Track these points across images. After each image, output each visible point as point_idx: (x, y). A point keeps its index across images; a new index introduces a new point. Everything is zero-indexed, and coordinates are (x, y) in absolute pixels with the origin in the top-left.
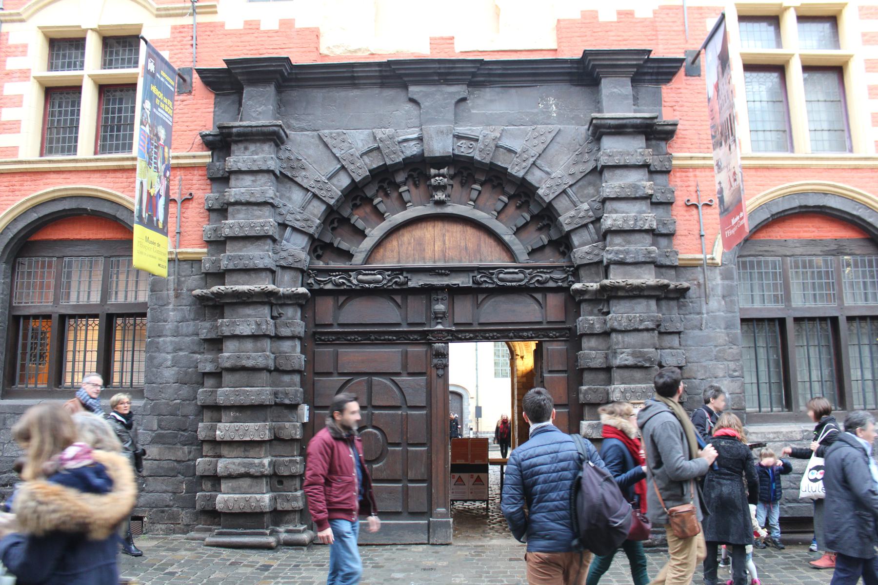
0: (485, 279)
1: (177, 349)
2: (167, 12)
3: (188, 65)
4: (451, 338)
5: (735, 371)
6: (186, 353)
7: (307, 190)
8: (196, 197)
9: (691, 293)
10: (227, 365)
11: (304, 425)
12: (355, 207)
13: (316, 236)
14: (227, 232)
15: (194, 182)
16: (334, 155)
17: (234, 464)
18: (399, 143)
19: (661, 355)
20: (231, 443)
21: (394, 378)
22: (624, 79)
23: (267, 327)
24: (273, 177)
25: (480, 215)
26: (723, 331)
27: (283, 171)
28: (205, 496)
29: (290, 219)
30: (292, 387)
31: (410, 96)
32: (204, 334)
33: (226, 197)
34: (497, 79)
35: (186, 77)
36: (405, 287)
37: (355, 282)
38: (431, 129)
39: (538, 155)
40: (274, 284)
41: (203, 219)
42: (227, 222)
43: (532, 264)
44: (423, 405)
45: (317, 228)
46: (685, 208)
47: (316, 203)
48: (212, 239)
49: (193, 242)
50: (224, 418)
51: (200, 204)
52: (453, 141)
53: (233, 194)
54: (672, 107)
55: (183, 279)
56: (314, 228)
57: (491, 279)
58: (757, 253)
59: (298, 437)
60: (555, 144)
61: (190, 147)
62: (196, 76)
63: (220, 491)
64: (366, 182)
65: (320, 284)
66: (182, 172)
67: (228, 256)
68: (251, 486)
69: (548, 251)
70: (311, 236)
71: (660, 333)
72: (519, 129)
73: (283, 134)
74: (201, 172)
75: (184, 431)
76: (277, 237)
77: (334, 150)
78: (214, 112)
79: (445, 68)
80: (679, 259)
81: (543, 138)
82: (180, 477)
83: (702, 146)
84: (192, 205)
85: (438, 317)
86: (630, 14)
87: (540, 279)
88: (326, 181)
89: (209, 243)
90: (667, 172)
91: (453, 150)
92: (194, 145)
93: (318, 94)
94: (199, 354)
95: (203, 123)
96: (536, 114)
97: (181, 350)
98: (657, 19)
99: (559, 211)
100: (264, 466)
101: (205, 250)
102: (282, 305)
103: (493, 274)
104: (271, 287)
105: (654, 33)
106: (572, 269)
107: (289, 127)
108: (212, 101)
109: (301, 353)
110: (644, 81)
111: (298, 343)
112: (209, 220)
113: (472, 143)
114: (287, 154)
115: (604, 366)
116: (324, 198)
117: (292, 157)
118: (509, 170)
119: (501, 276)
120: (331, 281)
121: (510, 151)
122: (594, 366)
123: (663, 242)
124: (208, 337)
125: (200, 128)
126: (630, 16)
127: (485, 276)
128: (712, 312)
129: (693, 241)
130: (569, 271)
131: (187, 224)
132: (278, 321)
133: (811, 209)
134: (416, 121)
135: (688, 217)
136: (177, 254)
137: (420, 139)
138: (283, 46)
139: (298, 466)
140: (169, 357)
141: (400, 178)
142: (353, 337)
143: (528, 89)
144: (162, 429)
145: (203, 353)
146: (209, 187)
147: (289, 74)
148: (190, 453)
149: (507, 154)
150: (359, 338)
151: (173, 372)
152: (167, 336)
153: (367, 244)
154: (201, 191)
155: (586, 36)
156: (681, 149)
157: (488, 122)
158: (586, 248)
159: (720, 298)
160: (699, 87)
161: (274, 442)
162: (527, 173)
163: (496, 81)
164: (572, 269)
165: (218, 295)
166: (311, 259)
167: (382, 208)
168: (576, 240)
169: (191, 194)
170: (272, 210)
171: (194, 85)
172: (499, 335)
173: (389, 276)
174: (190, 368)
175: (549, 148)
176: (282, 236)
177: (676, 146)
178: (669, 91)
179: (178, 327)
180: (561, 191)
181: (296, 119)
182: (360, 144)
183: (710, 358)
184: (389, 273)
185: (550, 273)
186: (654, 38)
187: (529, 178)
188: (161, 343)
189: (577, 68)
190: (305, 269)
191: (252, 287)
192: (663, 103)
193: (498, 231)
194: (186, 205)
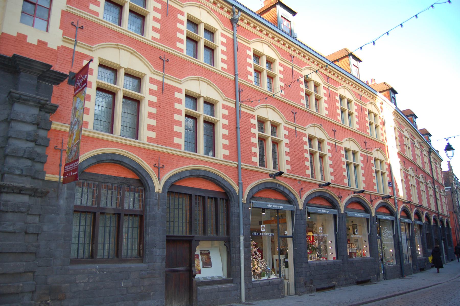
54: (57, 97)
58: (87, 179)
86: (45, 44)
98: (59, 51)
126: (45, 45)
155: (17, 47)
156: (57, 120)
186: (55, 60)
192: (53, 94)
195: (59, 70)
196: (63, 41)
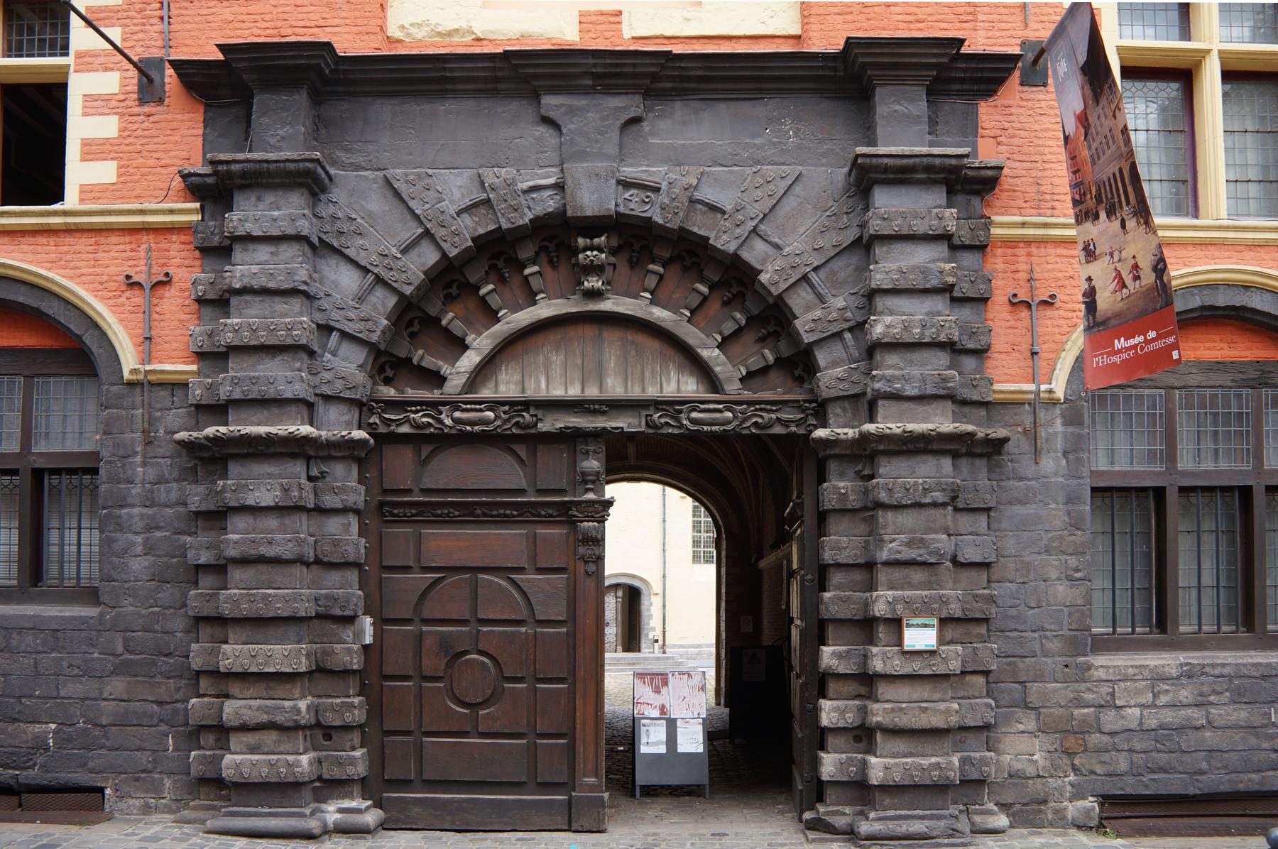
1: (149, 529)
3: (156, 53)
5: (1078, 570)
6: (168, 534)
7: (365, 270)
8: (175, 279)
11: (366, 648)
13: (382, 347)
14: (229, 338)
16: (411, 211)
17: (250, 708)
18: (524, 192)
20: (244, 677)
23: (301, 493)
24: (307, 249)
25: (660, 314)
26: (1061, 506)
27: (324, 237)
28: (205, 756)
29: (337, 318)
30: (346, 588)
31: (543, 112)
32: (195, 503)
33: (227, 281)
34: (693, 85)
35: (154, 75)
36: (533, 431)
38: (578, 169)
40: (312, 425)
44: (561, 618)
45: (383, 332)
47: (380, 293)
48: (206, 349)
49: (174, 354)
50: (231, 636)
53: (238, 275)
55: (159, 414)
57: (677, 420)
59: (355, 667)
61: (165, 194)
62: (169, 71)
63: (228, 750)
64: (468, 258)
65: (389, 426)
66: (151, 237)
67: (233, 378)
68: (278, 742)
71: (956, 510)
72: (731, 172)
73: (323, 175)
74: (183, 238)
75: (166, 655)
76: (315, 348)
77: (412, 204)
78: (204, 135)
79: (604, 65)
80: (994, 392)
81: (771, 186)
82: (164, 728)
83: (1043, 205)
87: (760, 420)
88: (399, 256)
89: (201, 356)
90: (981, 248)
91: (617, 205)
92: (170, 192)
93: (384, 110)
94: (190, 534)
95: (184, 154)
96: (760, 147)
97: (158, 528)
99: (796, 310)
100: (299, 711)
102: (330, 458)
103: (680, 412)
104: (306, 430)
107: (334, 163)
108: (199, 116)
109: (360, 535)
110: (948, 93)
111: (354, 521)
112: (199, 318)
113: (649, 194)
114: (332, 209)
115: (861, 561)
116: (393, 284)
117: (340, 215)
118: (711, 242)
119: (694, 415)
120: (408, 421)
121: (714, 209)
122: (845, 561)
124: (202, 508)
125: (180, 163)
127: (667, 416)
128: (1045, 477)
129: (1018, 362)
130: (808, 408)
132: (319, 484)
133: (1220, 313)
134: (553, 156)
136: (147, 372)
137: (560, 187)
138: (322, 23)
139: (356, 712)
140: (139, 539)
141: (525, 253)
143: (746, 105)
144: (131, 652)
145: (196, 533)
146: (198, 263)
147: (332, 71)
148: (178, 689)
149: (710, 215)
150: (457, 513)
151: (147, 564)
152: (134, 506)
153: (469, 360)
157: (677, 159)
158: (839, 371)
159: (1059, 454)
160: (1043, 104)
161: (317, 675)
165: (216, 440)
167: (494, 301)
168: (822, 357)
169: (167, 275)
171: (167, 88)
173: (505, 413)
174: (173, 557)
175: (781, 204)
176: (324, 347)
178: (992, 110)
180: (799, 276)
181: (346, 150)
182: (457, 194)
183: (1036, 550)
184: (506, 408)
185: (777, 411)
187: (746, 255)
190: (364, 400)
191: (273, 430)
193: (691, 341)
194: (159, 292)
195: (987, 48)
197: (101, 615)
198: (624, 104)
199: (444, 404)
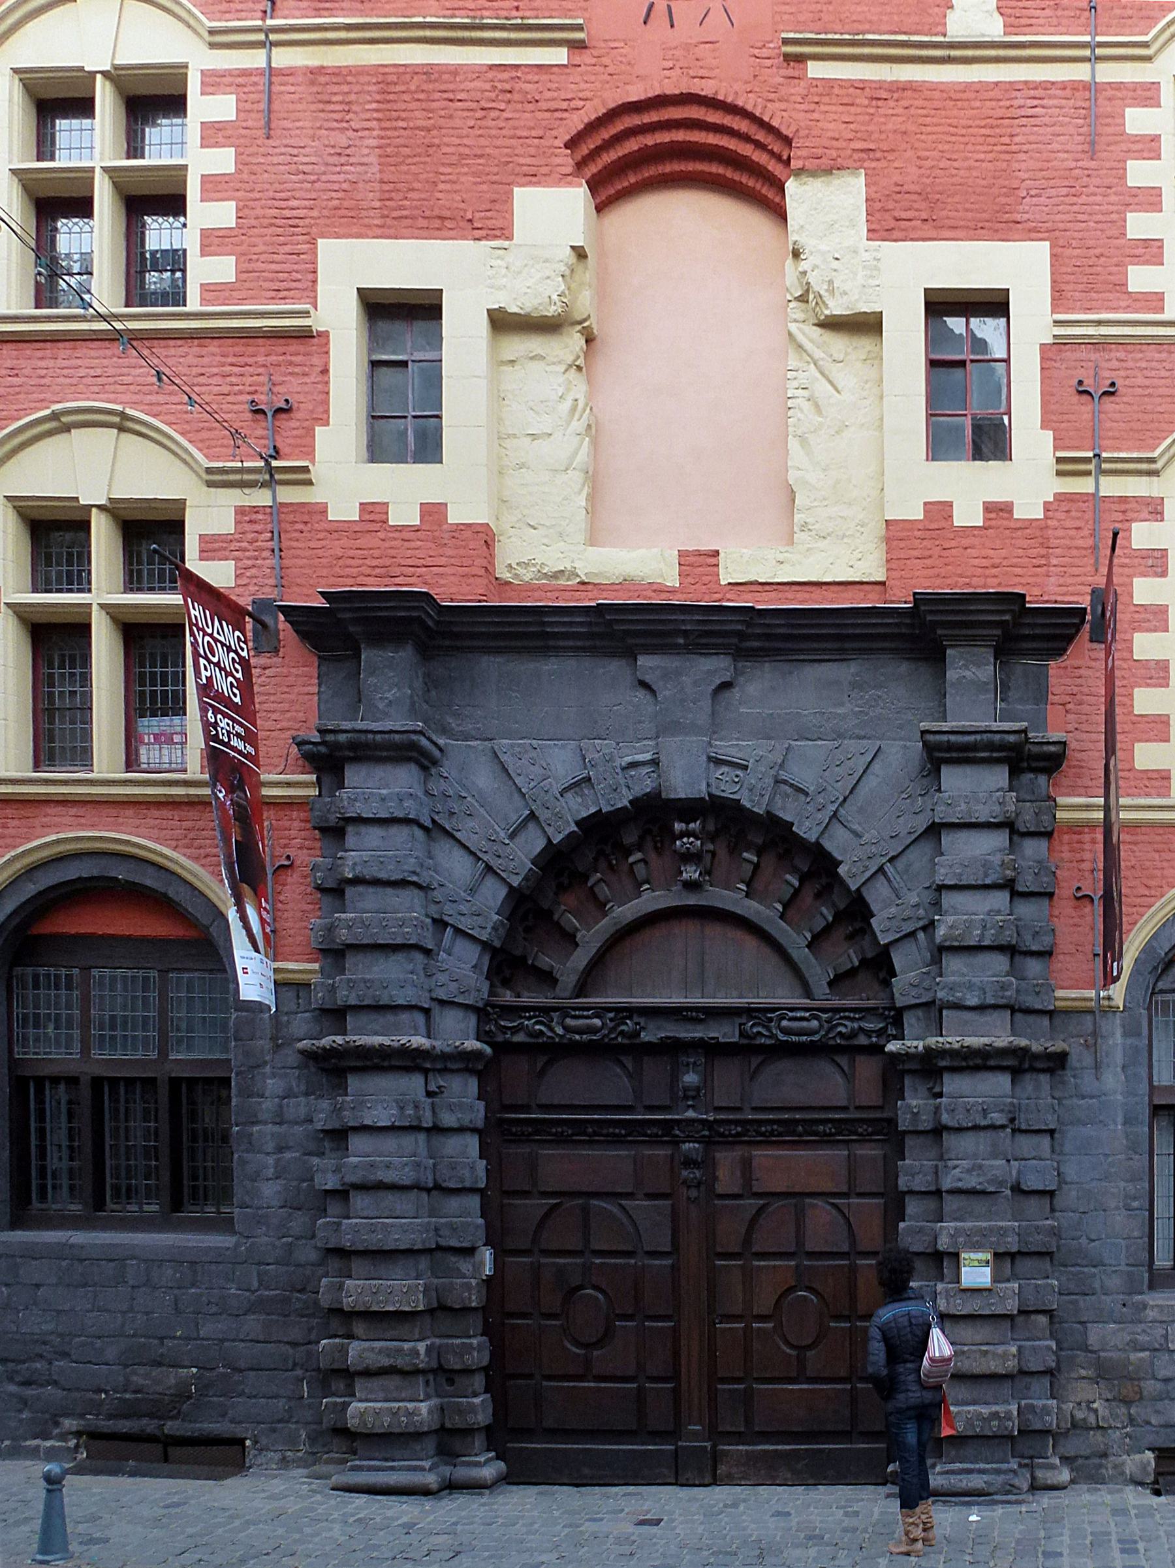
0: (760, 1029)
2: (225, 477)
4: (707, 1133)
9: (1073, 1060)
10: (351, 1178)
12: (561, 888)
15: (293, 833)
18: (623, 769)
19: (1019, 1172)
21: (623, 1202)
22: (983, 650)
27: (436, 818)
28: (336, 1404)
29: (450, 912)
36: (637, 1041)
37: (560, 1030)
38: (671, 743)
39: (841, 799)
41: (311, 907)
42: (343, 916)
43: (837, 1003)
45: (494, 928)
46: (1074, 902)
47: (490, 882)
49: (299, 950)
51: (305, 877)
52: (707, 768)
56: (489, 930)
57: (768, 1029)
59: (474, 1304)
60: (872, 777)
65: (505, 1033)
69: (862, 977)
70: (485, 945)
74: (302, 815)
84: (292, 878)
85: (693, 1095)
88: (507, 841)
93: (491, 666)
97: (288, 1148)
98: (1049, 522)
99: (874, 907)
100: (418, 1354)
101: (316, 966)
103: (771, 1020)
105: (1043, 551)
106: (892, 1013)
107: (445, 731)
114: (443, 785)
119: (784, 1023)
123: (1033, 967)
126: (1005, 515)
127: (759, 1024)
131: (286, 915)
135: (1076, 920)
140: (271, 1161)
142: (560, 1130)
146: (318, 844)
152: (265, 1123)
154: (305, 851)
156: (1073, 791)
162: (822, 833)
163: (780, 649)
164: (892, 1013)
166: (492, 986)
170: (422, 894)
172: (781, 1129)
173: (611, 1020)
176: (439, 944)
177: (1065, 782)
179: (281, 1106)
181: (457, 715)
188: (256, 1135)
189: (911, 626)
192: (1050, 696)
196: (1059, 473)
197: (237, 1245)
198: (717, 666)
199: (555, 1009)
